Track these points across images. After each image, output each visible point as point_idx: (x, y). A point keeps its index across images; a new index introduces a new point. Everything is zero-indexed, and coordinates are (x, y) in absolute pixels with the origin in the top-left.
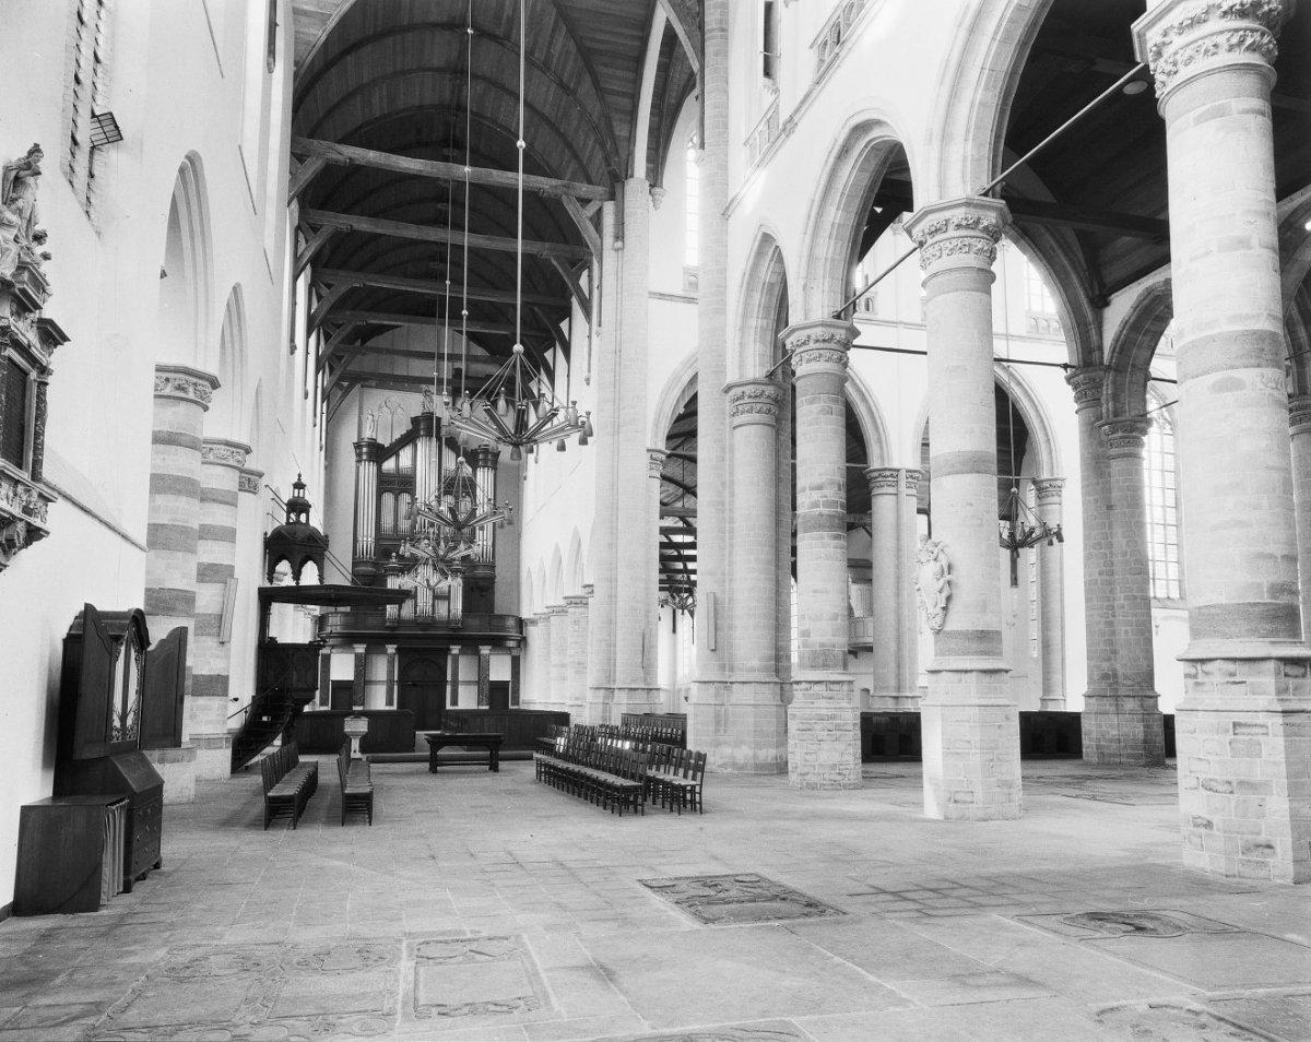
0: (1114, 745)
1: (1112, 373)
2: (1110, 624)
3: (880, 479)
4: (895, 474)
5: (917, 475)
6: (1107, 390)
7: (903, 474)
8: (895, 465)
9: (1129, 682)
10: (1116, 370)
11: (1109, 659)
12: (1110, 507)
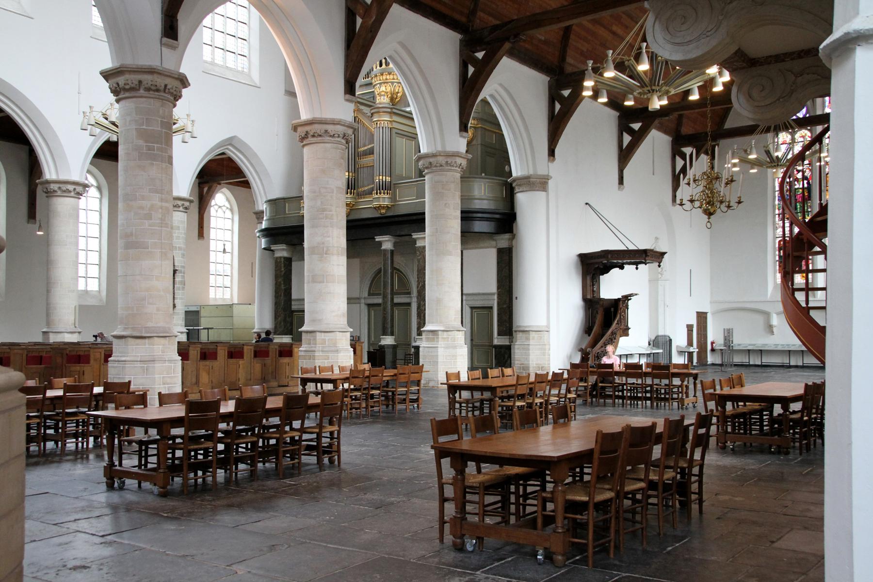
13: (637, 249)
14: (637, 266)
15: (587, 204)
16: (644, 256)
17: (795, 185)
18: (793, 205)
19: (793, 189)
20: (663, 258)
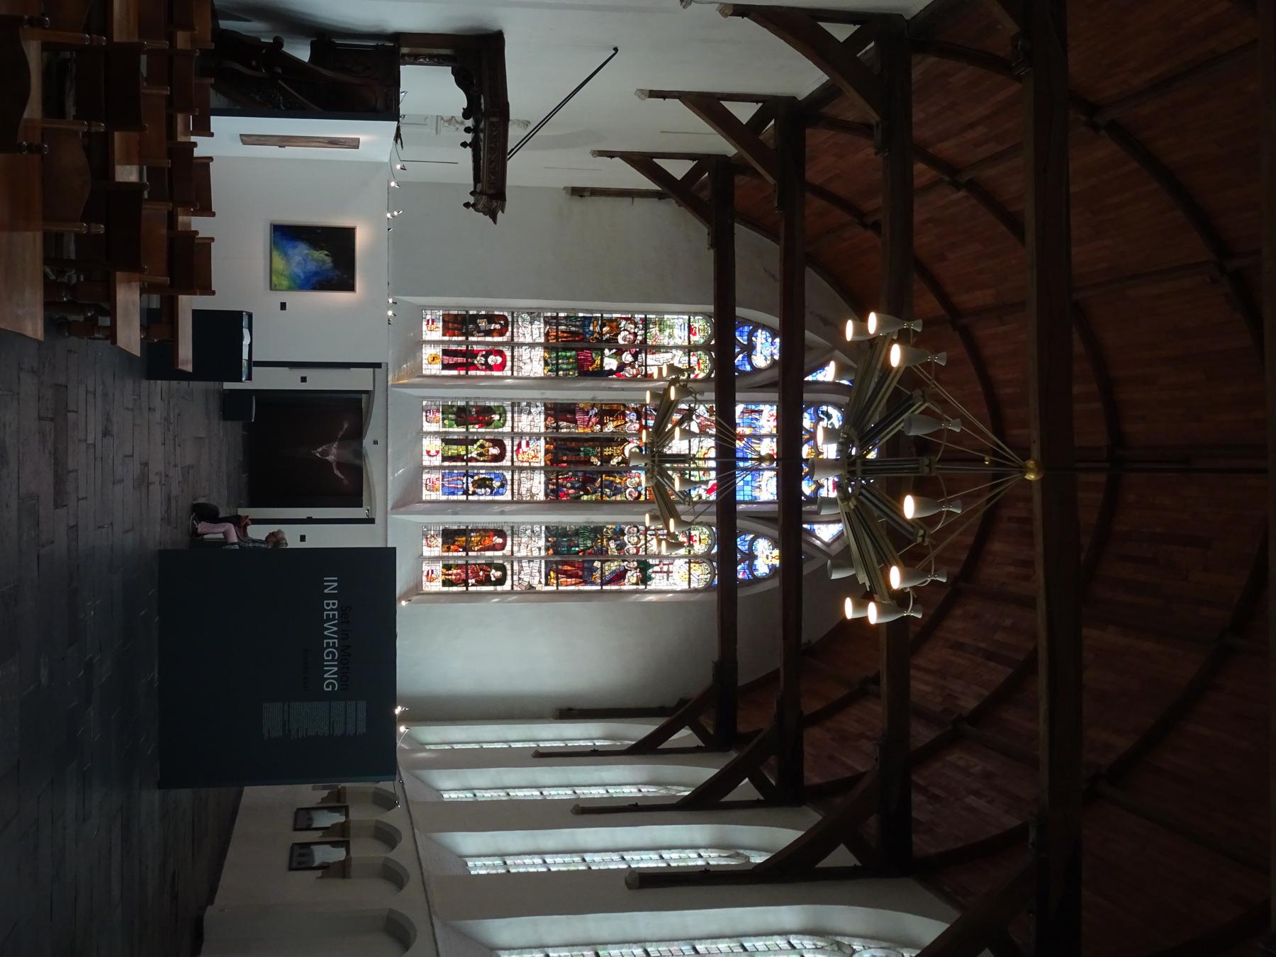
13: (511, 145)
14: (470, 145)
15: (616, 49)
16: (492, 191)
17: (610, 350)
18: (573, 345)
19: (603, 345)
20: (485, 214)
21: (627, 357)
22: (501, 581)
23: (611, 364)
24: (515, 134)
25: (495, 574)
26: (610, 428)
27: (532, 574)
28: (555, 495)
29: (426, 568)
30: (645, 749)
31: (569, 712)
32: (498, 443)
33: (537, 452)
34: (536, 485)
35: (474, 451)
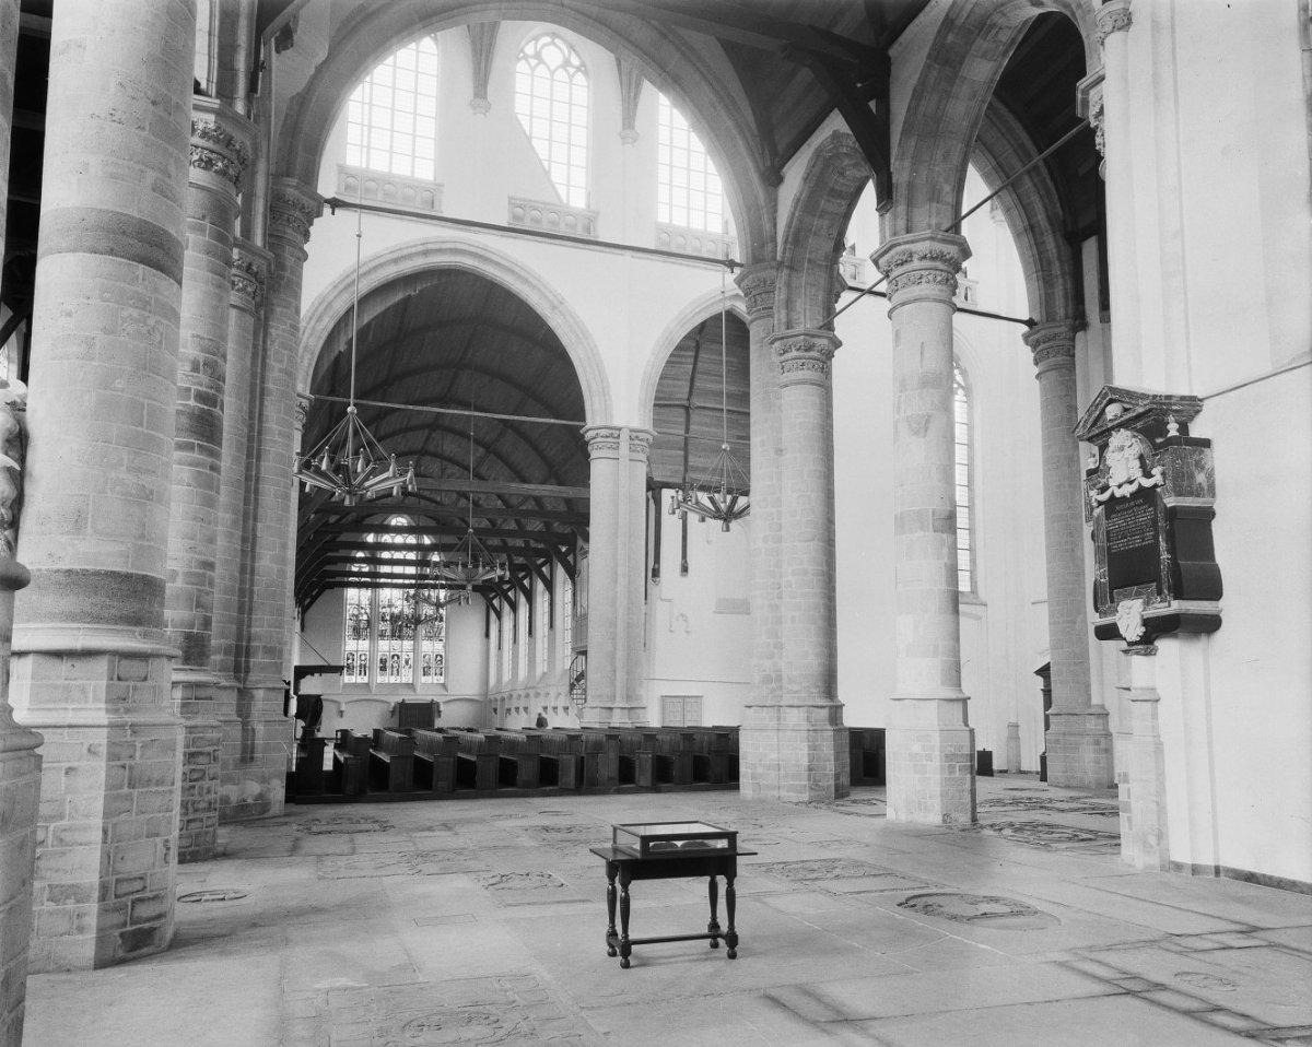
0: (773, 774)
1: (786, 271)
2: (777, 607)
3: (598, 440)
4: (616, 433)
5: (641, 435)
6: (780, 296)
7: (624, 436)
8: (617, 422)
9: (796, 688)
10: (788, 267)
11: (771, 656)
12: (779, 452)
21: (363, 611)
22: (441, 656)
23: (365, 617)
24: (325, 664)
25: (439, 658)
26: (388, 618)
27: (439, 647)
28: (414, 638)
29: (435, 682)
30: (499, 616)
31: (487, 635)
32: (393, 656)
33: (396, 643)
34: (408, 644)
35: (395, 665)
